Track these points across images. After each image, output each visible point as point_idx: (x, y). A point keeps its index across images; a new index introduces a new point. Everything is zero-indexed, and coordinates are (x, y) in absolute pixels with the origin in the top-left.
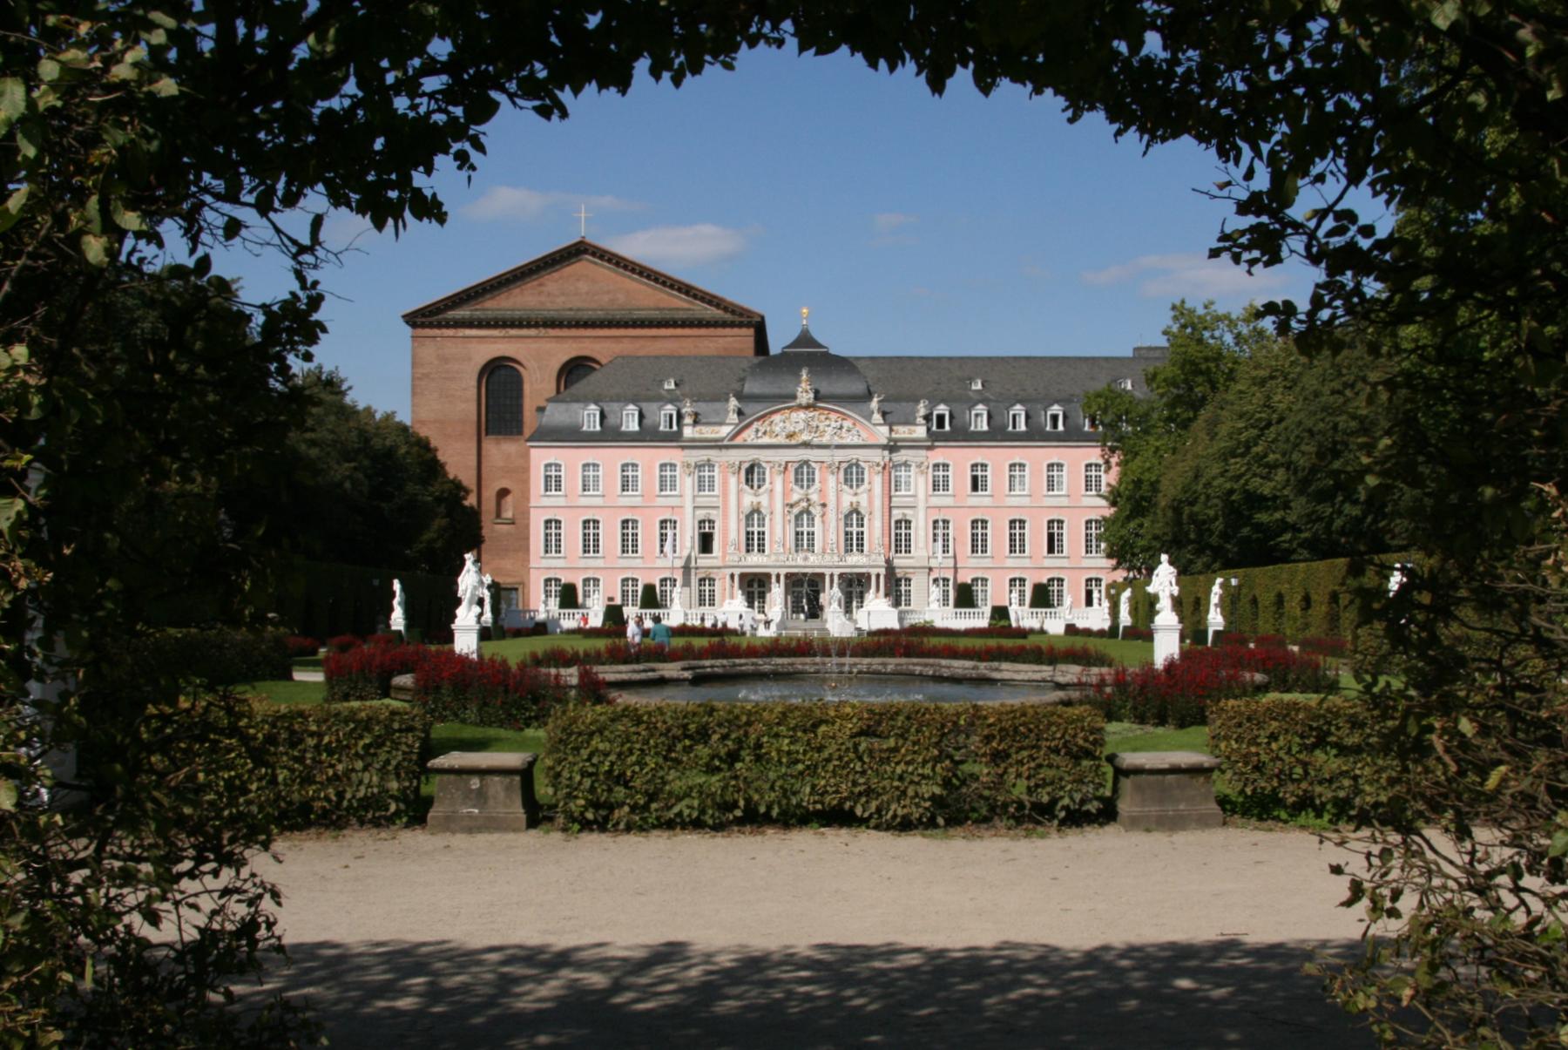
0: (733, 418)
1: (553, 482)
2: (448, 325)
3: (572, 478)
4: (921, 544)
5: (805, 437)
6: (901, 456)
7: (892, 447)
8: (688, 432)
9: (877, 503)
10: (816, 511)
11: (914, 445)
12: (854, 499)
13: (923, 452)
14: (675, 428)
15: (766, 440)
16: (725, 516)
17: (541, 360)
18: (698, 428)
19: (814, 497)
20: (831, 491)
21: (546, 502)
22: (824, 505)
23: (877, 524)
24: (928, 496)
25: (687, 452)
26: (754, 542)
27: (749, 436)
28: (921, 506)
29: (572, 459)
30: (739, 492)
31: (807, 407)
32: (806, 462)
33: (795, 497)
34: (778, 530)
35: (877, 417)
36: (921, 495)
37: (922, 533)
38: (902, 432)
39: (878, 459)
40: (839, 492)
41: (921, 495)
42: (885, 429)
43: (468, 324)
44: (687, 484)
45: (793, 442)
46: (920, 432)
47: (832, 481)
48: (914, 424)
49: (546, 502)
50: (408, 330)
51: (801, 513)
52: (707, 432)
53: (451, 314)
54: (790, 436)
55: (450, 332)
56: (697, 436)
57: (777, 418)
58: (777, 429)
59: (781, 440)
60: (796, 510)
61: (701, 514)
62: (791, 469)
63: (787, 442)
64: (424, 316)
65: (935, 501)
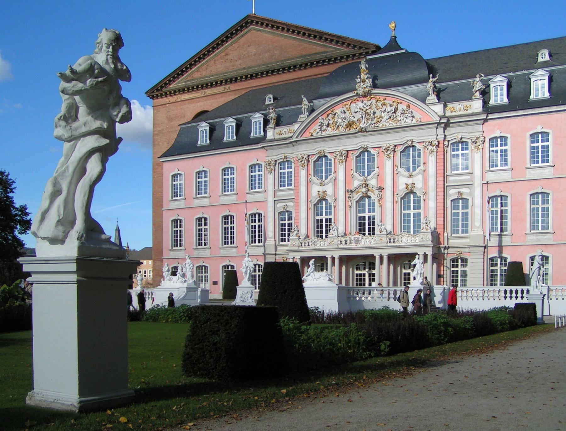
2: (175, 92)
3: (188, 183)
4: (477, 223)
5: (362, 125)
6: (454, 133)
7: (446, 123)
8: (270, 134)
9: (432, 182)
10: (374, 196)
11: (468, 120)
12: (410, 181)
13: (479, 128)
14: (262, 133)
15: (330, 131)
16: (297, 206)
18: (278, 130)
19: (373, 182)
20: (390, 176)
21: (173, 205)
22: (381, 189)
23: (432, 204)
24: (484, 172)
25: (269, 152)
26: (322, 228)
27: (315, 130)
28: (478, 182)
30: (309, 182)
32: (365, 150)
33: (356, 183)
34: (343, 219)
35: (432, 98)
36: (477, 171)
37: (478, 211)
38: (457, 108)
39: (432, 138)
40: (395, 174)
41: (477, 171)
42: (439, 108)
43: (182, 91)
44: (270, 180)
45: (352, 131)
46: (477, 105)
47: (389, 164)
48: (470, 99)
51: (362, 198)
52: (285, 131)
53: (173, 86)
54: (350, 125)
55: (172, 99)
56: (277, 137)
57: (338, 110)
59: (342, 130)
60: (356, 197)
61: (280, 205)
62: (352, 157)
64: (158, 90)
65: (491, 177)
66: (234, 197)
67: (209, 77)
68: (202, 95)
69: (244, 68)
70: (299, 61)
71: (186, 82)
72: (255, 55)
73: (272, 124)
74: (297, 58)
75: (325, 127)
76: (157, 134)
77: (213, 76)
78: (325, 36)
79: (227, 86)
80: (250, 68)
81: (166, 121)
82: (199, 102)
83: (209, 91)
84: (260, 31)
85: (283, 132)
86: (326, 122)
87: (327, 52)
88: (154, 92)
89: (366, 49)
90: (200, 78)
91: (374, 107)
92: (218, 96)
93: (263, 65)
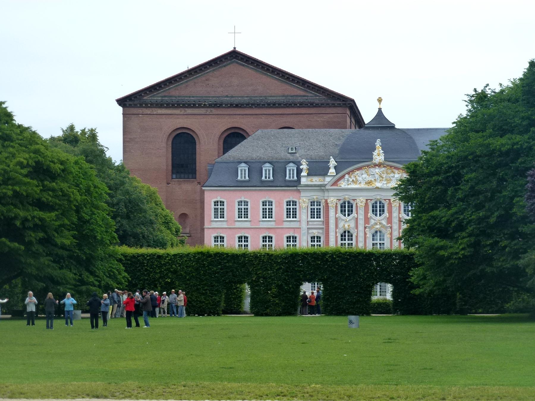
0: (332, 171)
1: (219, 213)
3: (231, 209)
8: (304, 181)
14: (295, 178)
17: (207, 130)
18: (310, 178)
29: (231, 199)
31: (379, 165)
43: (160, 105)
45: (370, 187)
49: (214, 225)
50: (121, 109)
52: (316, 180)
54: (369, 183)
55: (148, 111)
58: (360, 179)
59: (363, 186)
63: (367, 186)
64: (131, 100)
66: (273, 223)
67: (190, 97)
68: (182, 113)
69: (227, 96)
70: (282, 99)
71: (162, 97)
72: (238, 86)
73: (304, 173)
74: (279, 96)
75: (349, 183)
76: (128, 142)
77: (193, 97)
78: (308, 84)
79: (209, 110)
80: (232, 97)
81: (139, 130)
82: (178, 118)
83: (189, 111)
84: (243, 65)
85: (314, 180)
86: (351, 180)
87: (308, 96)
88: (126, 101)
89: (343, 101)
90: (179, 97)
91: (385, 172)
92: (199, 117)
93: (247, 97)
